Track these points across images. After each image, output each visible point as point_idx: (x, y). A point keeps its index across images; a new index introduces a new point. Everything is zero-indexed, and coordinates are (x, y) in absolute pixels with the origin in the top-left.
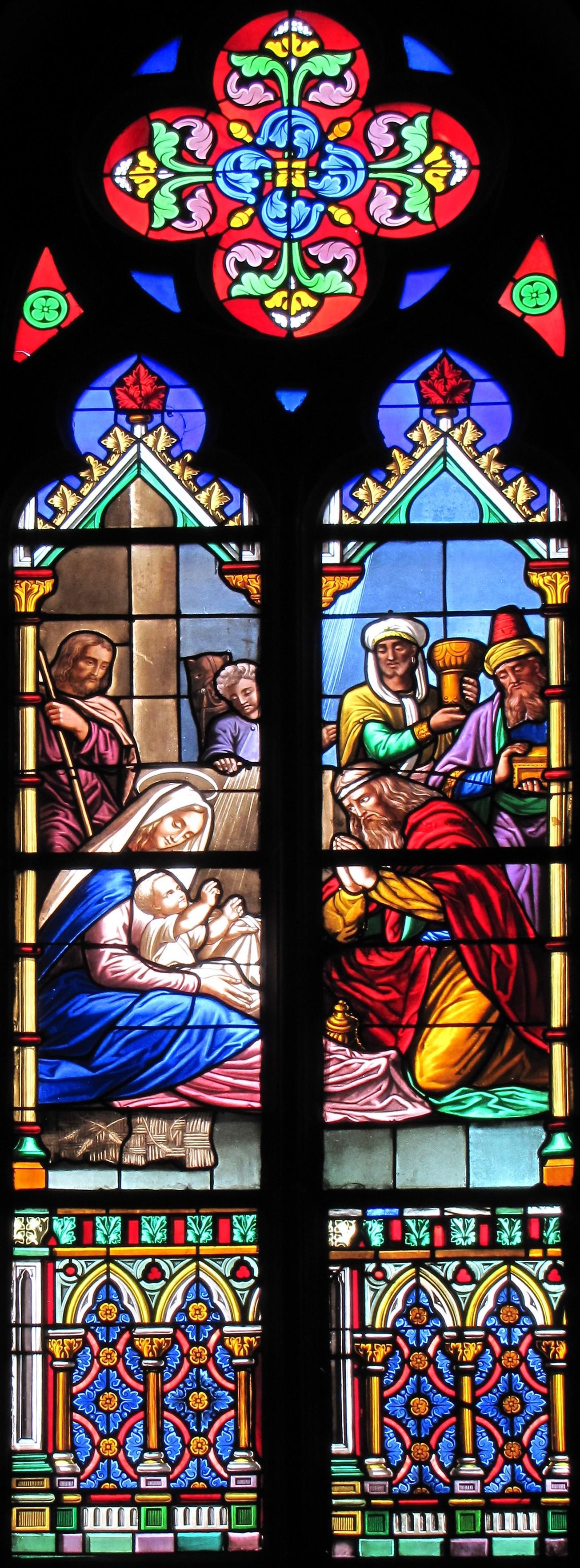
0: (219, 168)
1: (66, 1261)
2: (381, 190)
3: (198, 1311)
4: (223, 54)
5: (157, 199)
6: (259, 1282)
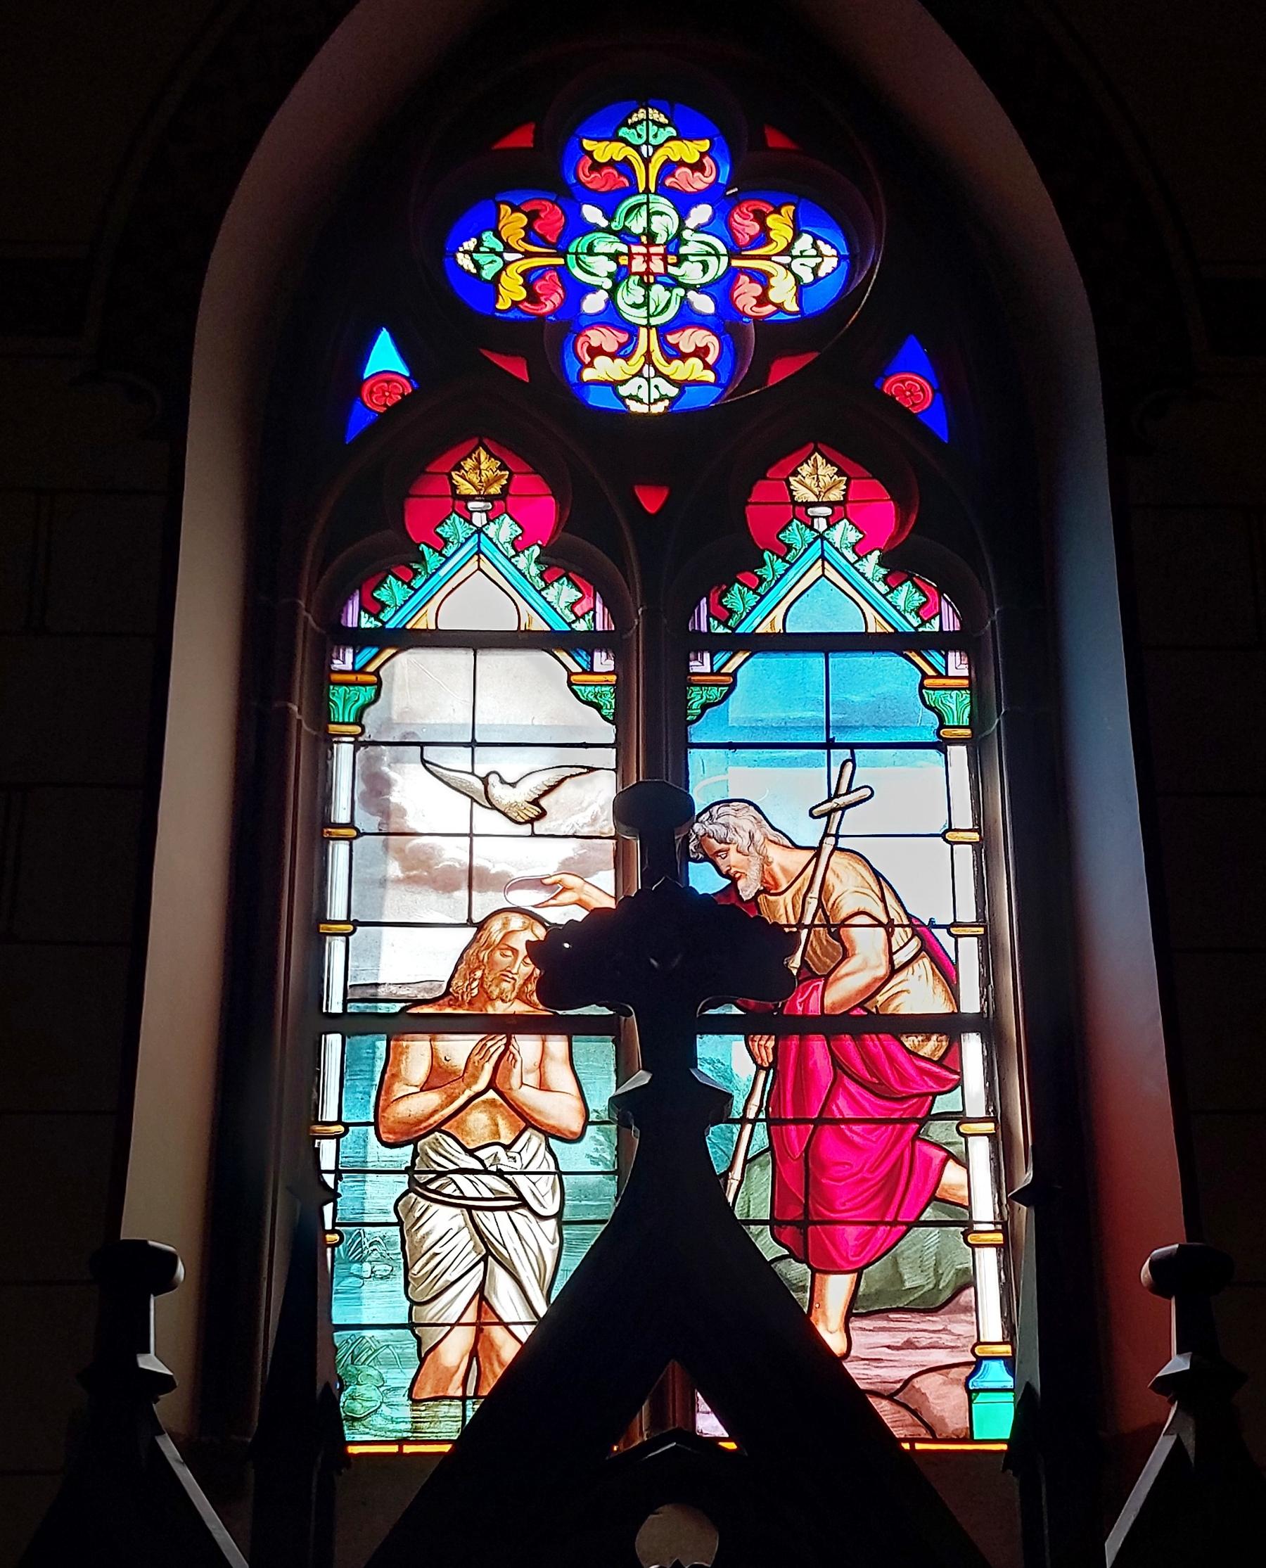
0: (572, 249)
2: (744, 279)
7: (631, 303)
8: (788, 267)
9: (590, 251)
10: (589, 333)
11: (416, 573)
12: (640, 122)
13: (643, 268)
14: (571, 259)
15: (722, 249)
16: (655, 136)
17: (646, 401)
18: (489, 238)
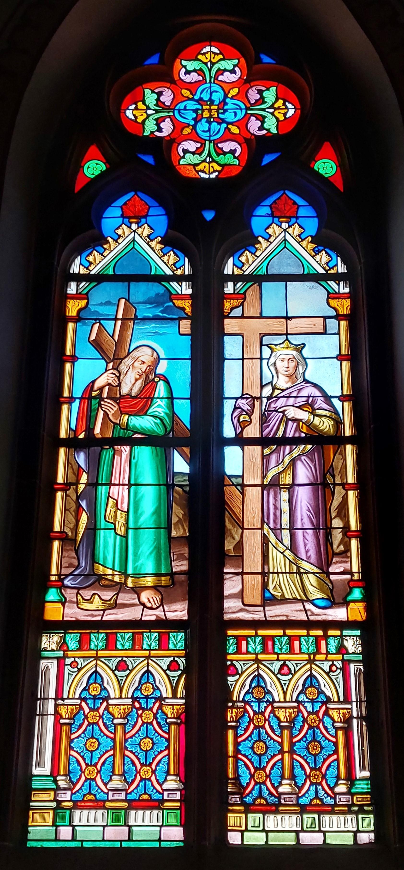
1: (73, 659)
2: (253, 118)
3: (148, 690)
4: (178, 60)
5: (147, 123)
6: (183, 672)
7: (202, 130)
8: (272, 114)
9: (185, 109)
10: (184, 143)
11: (105, 249)
12: (207, 52)
13: (208, 115)
14: (176, 112)
15: (243, 107)
16: (214, 58)
17: (207, 172)
18: (140, 105)
